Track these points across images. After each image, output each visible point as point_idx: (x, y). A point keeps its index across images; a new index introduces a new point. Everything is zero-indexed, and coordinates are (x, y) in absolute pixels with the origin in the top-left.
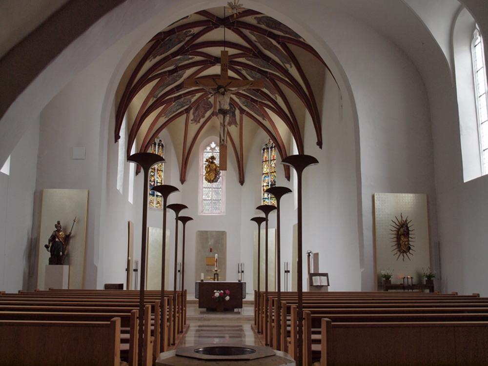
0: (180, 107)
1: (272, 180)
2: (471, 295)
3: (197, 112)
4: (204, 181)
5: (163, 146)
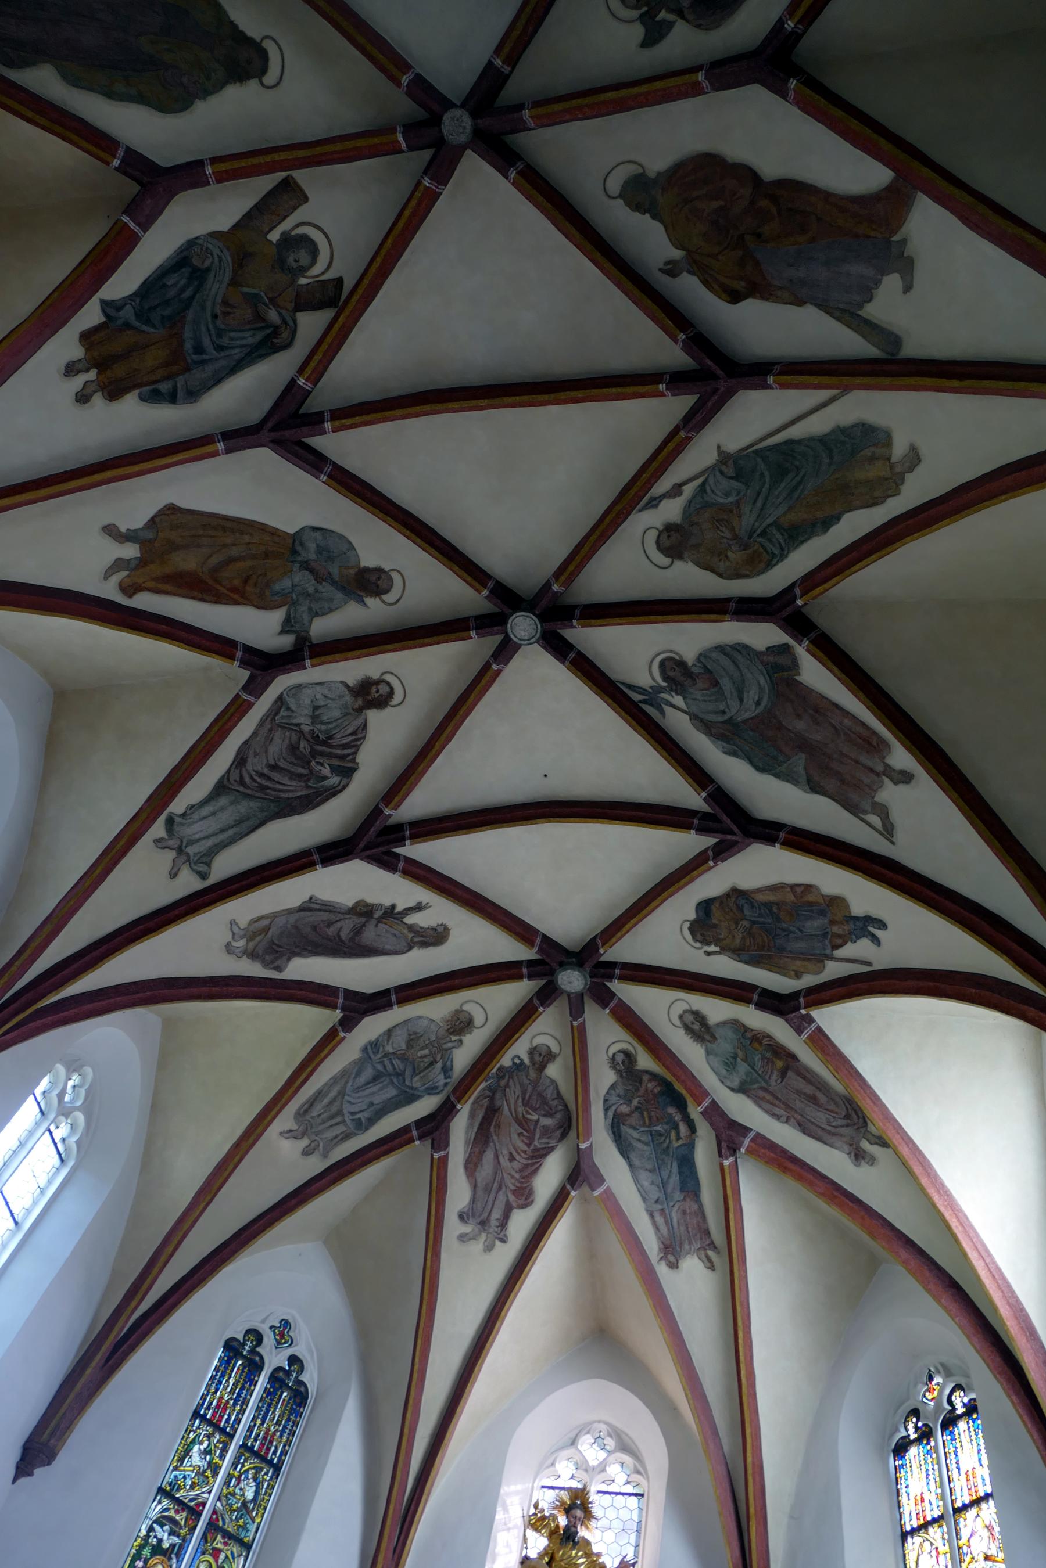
0: (391, 1092)
3: (489, 1156)
5: (300, 1396)
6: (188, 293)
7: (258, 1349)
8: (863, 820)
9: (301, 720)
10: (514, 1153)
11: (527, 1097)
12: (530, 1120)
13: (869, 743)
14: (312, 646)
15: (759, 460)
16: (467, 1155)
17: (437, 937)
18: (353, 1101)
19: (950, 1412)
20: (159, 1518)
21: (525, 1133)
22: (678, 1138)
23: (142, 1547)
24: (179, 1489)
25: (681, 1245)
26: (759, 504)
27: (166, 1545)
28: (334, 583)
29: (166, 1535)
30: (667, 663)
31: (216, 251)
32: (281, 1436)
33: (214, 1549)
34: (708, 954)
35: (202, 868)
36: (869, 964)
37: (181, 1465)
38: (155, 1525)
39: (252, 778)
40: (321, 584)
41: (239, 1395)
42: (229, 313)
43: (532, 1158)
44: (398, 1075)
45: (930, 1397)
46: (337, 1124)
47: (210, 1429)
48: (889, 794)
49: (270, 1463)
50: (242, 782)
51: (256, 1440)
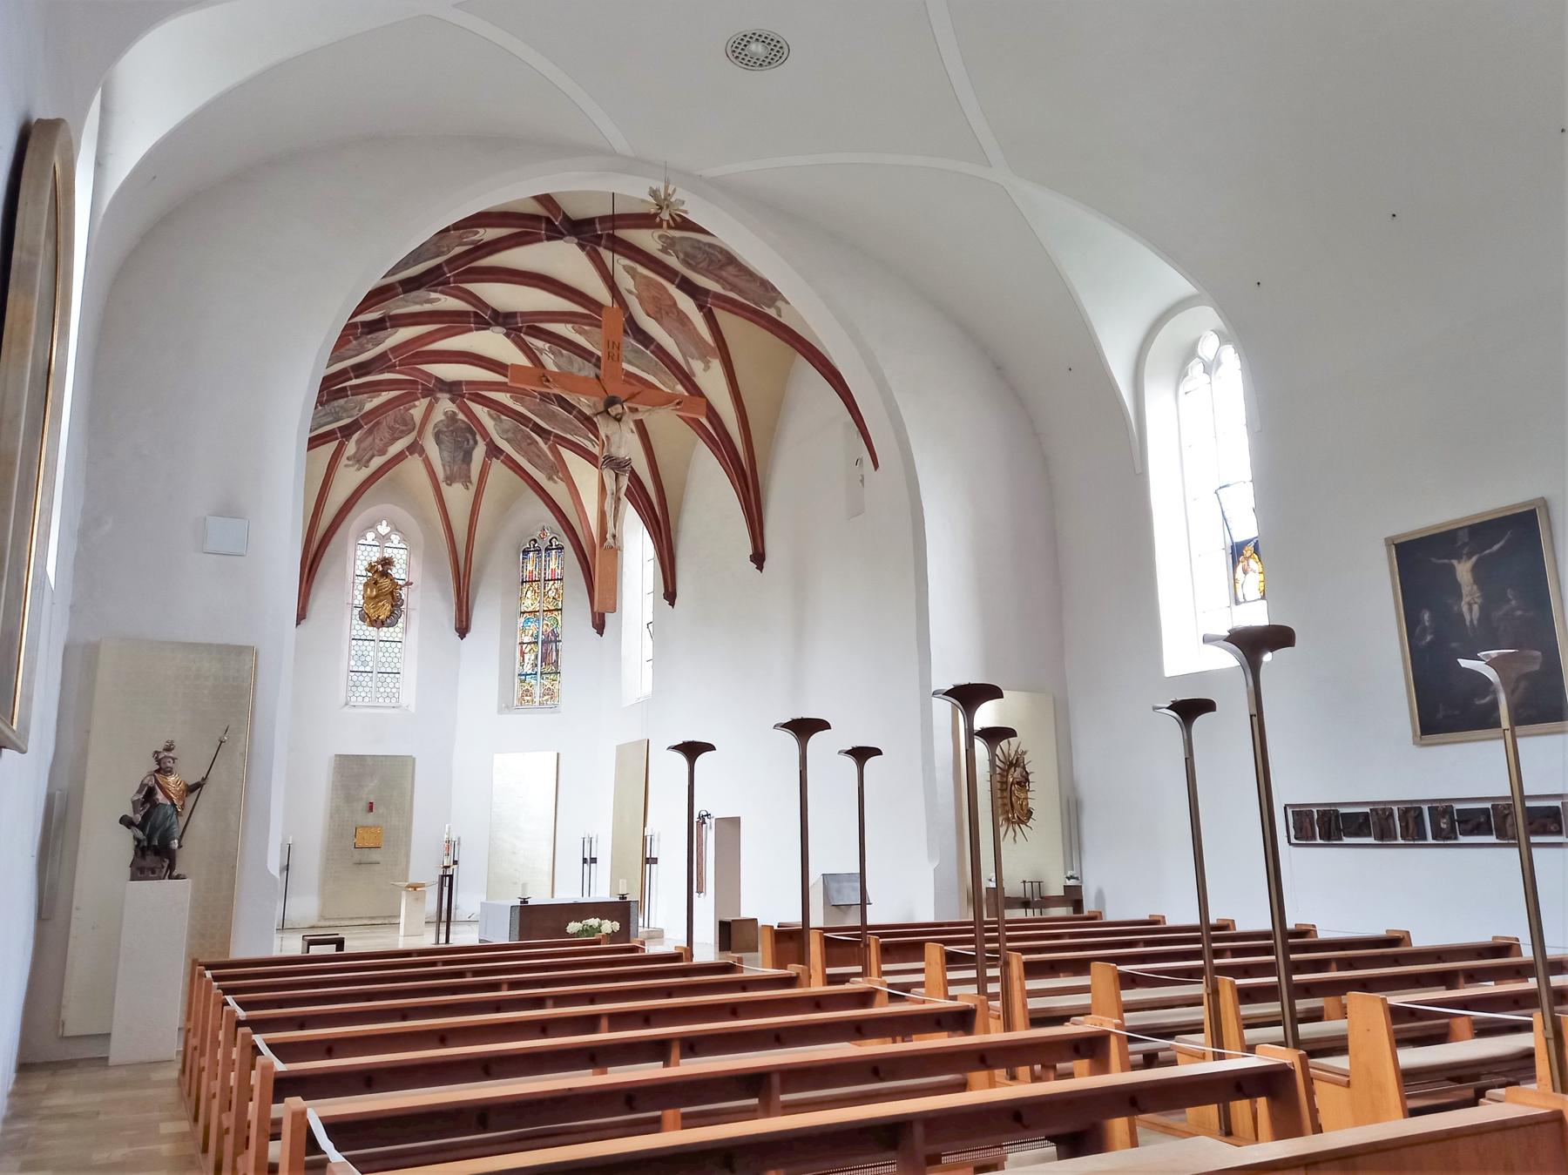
0: (331, 419)
1: (549, 630)
2: (1147, 918)
3: (370, 438)
4: (356, 621)
22: (468, 444)
25: (455, 479)
44: (336, 412)
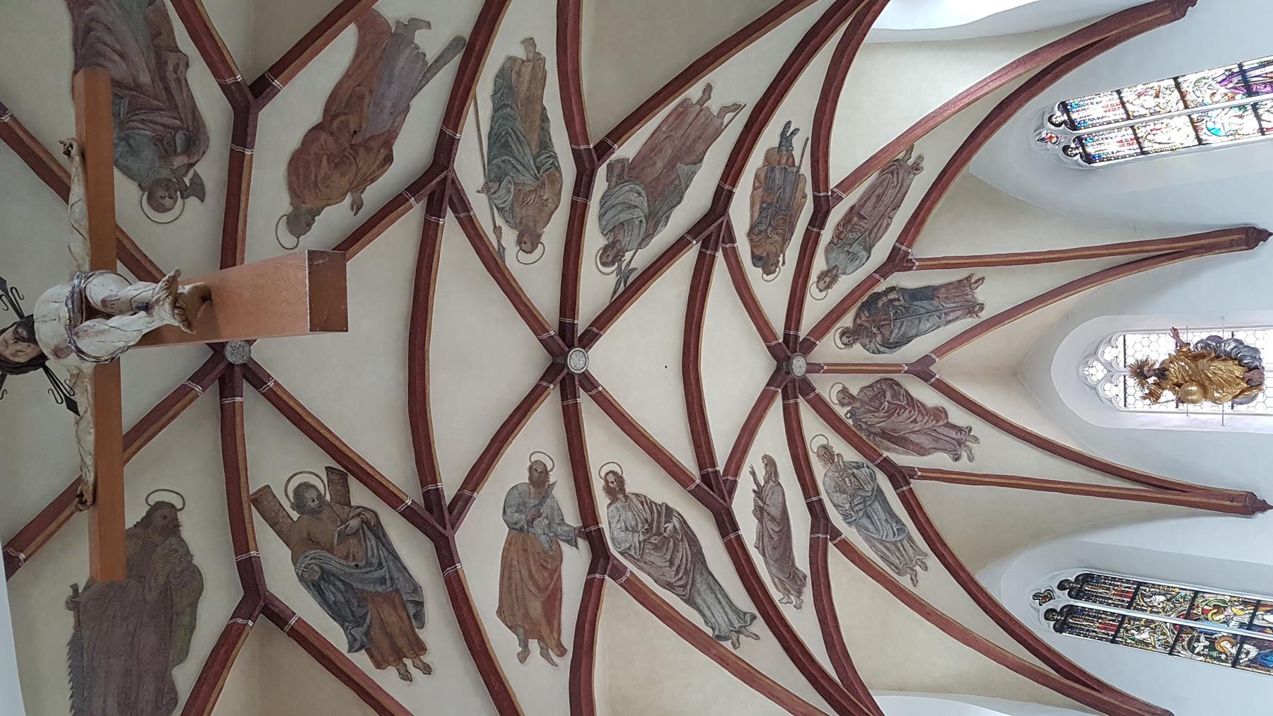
0: (877, 506)
3: (913, 437)
4: (1257, 405)
5: (1086, 578)
6: (340, 585)
7: (1058, 611)
8: (726, 126)
9: (636, 540)
10: (911, 419)
11: (873, 409)
12: (888, 407)
13: (682, 112)
14: (585, 526)
15: (494, 162)
16: (915, 454)
17: (770, 463)
18: (886, 534)
19: (1066, 125)
20: (1190, 651)
21: (897, 411)
22: (898, 300)
23: (1211, 657)
24: (1168, 642)
26: (520, 168)
27: (1207, 643)
28: (541, 503)
29: (1200, 644)
30: (603, 261)
31: (307, 561)
32: (1118, 586)
33: (1203, 614)
34: (784, 263)
35: (748, 618)
36: (808, 139)
37: (1151, 644)
38: (1195, 652)
39: (680, 579)
40: (542, 514)
41: (1094, 617)
42: (354, 556)
43: (914, 407)
45: (1056, 139)
46: (903, 546)
47: (1122, 630)
48: (714, 105)
49: (1137, 589)
50: (684, 586)
51: (1123, 601)
